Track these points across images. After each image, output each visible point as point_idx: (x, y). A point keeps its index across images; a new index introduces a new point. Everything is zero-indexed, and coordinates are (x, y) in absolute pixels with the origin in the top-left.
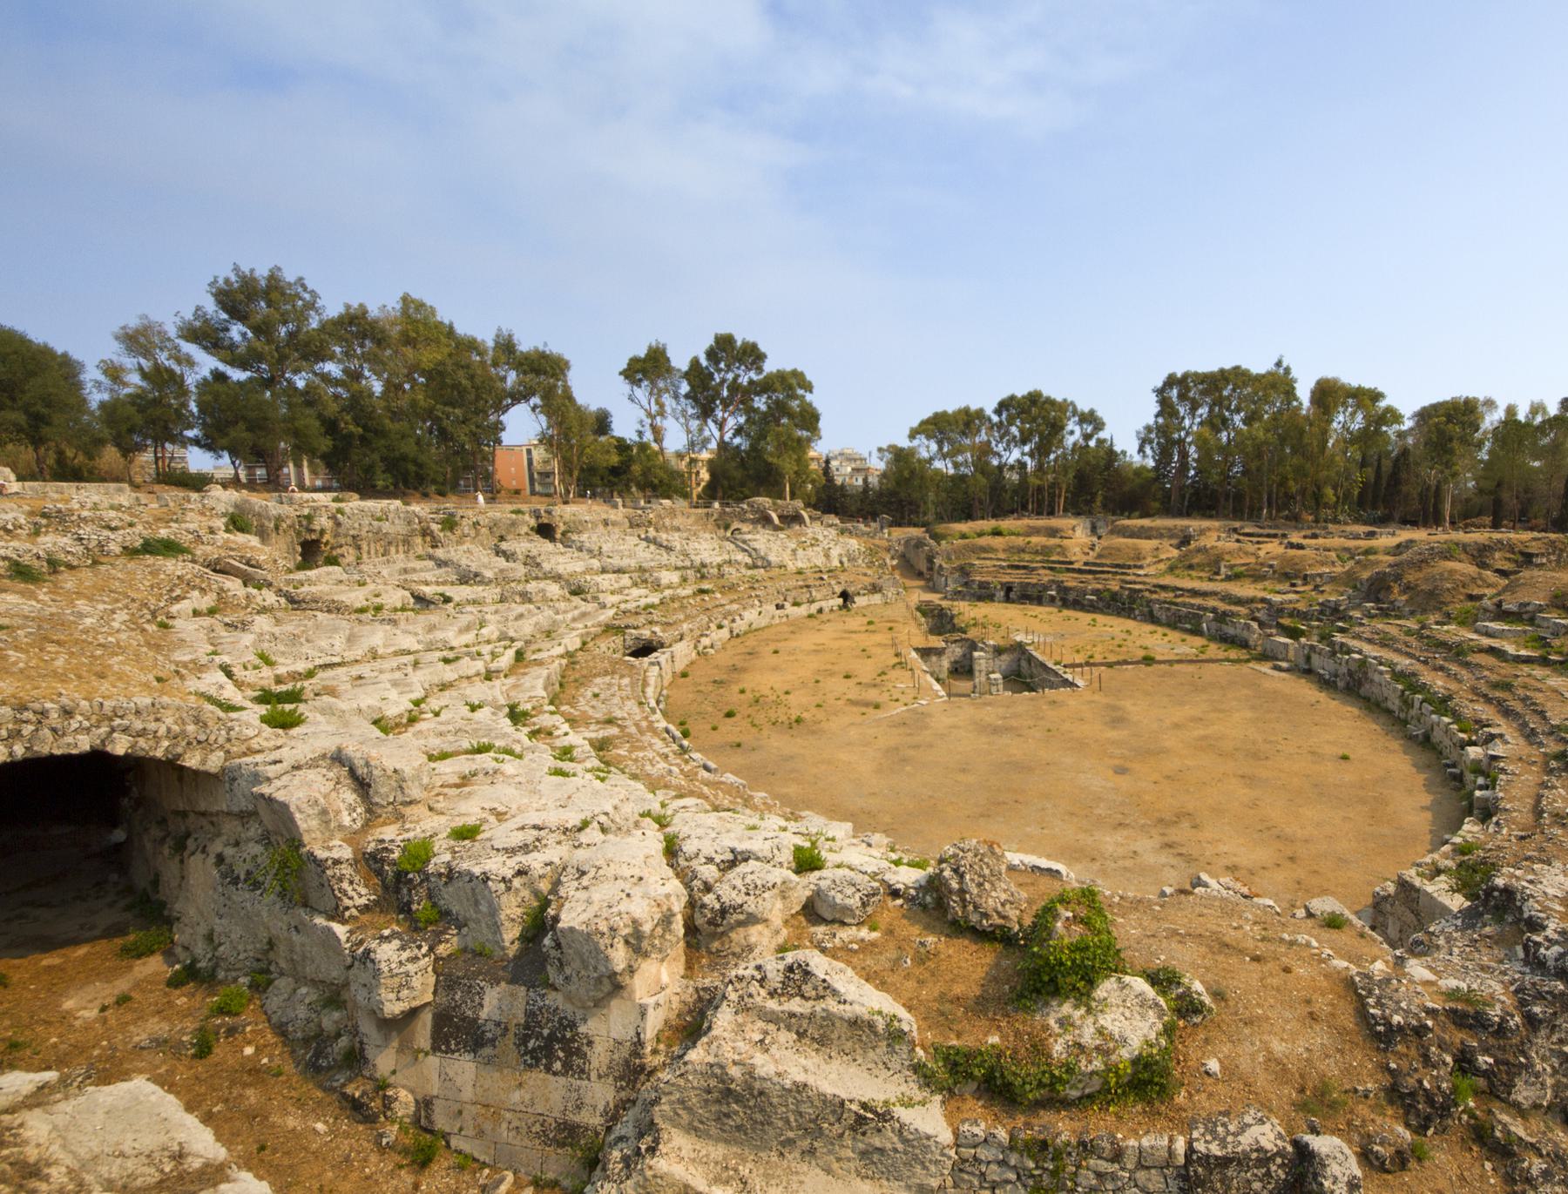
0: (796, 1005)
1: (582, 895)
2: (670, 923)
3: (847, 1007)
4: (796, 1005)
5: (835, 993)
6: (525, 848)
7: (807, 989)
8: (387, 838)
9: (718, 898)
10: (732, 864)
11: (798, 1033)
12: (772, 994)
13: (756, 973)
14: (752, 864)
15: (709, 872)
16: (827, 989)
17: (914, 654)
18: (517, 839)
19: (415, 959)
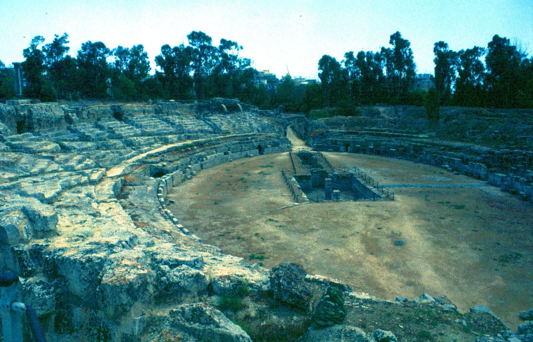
0: (196, 325)
1: (111, 271)
2: (146, 286)
3: (220, 329)
4: (196, 325)
5: (214, 322)
6: (91, 251)
7: (202, 319)
8: (40, 244)
9: (168, 279)
10: (177, 265)
11: (198, 338)
12: (188, 320)
13: (181, 310)
14: (184, 266)
15: (165, 268)
16: (210, 321)
17: (294, 179)
18: (88, 247)
19: (48, 294)
